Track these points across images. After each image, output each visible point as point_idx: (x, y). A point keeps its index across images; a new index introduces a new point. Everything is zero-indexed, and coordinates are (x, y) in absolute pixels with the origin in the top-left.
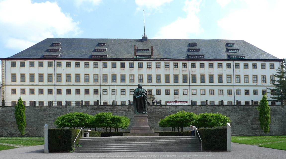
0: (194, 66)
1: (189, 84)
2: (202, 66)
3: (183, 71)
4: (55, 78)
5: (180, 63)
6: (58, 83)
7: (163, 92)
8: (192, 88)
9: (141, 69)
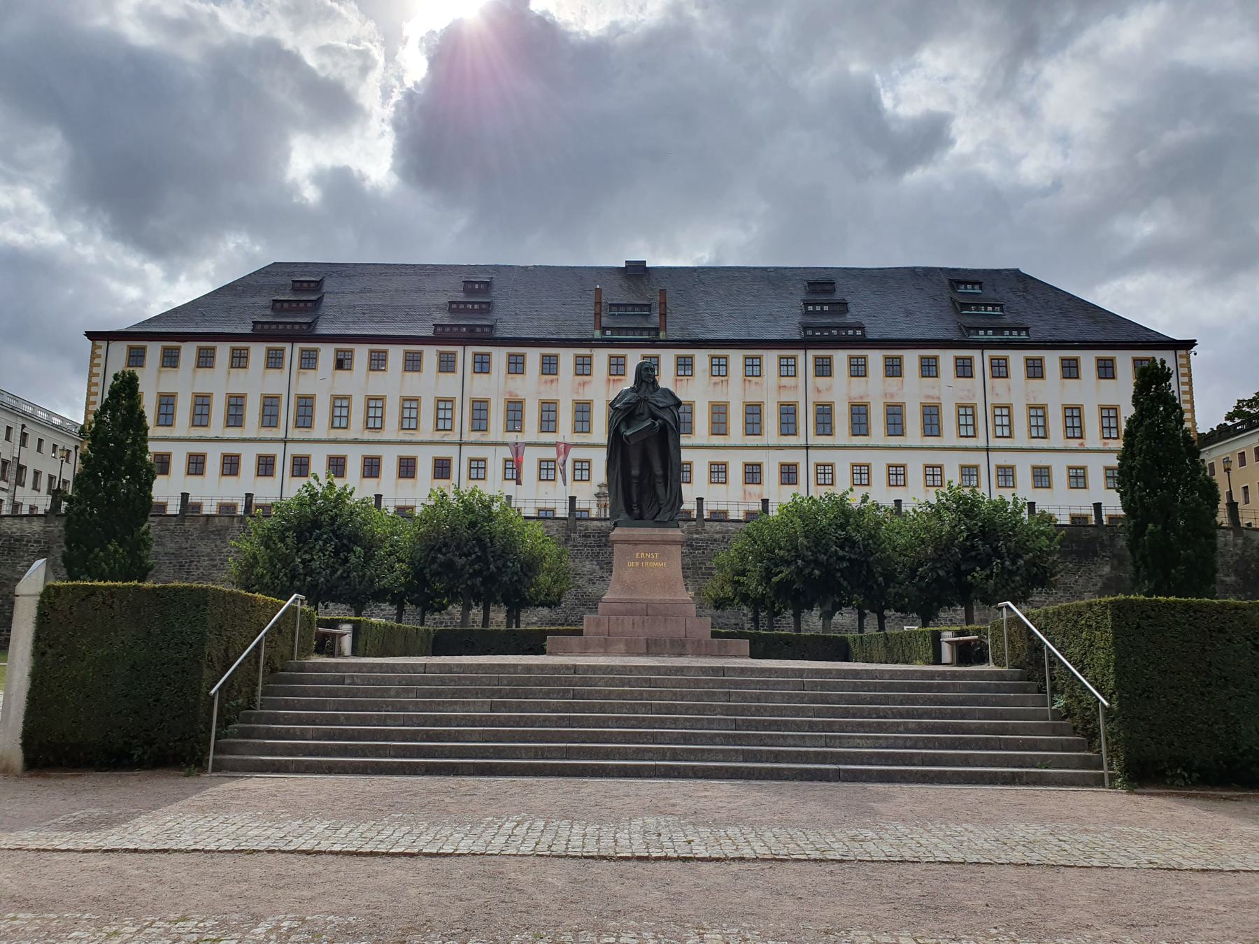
0: (824, 368)
1: (803, 442)
3: (780, 387)
4: (287, 412)
5: (770, 359)
6: (297, 431)
8: (817, 456)
9: (620, 380)
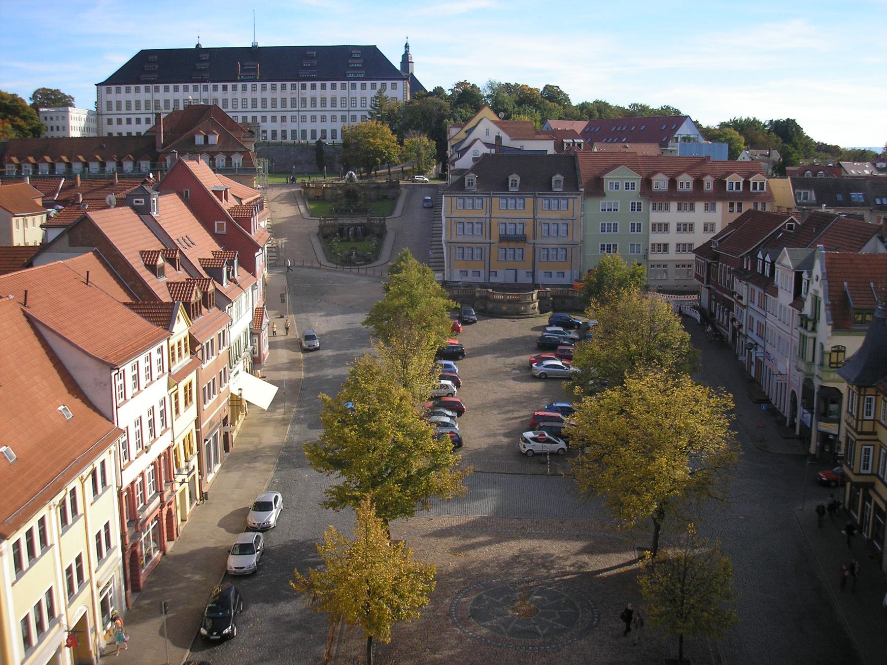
2: (313, 87)
7: (269, 119)
8: (301, 114)
